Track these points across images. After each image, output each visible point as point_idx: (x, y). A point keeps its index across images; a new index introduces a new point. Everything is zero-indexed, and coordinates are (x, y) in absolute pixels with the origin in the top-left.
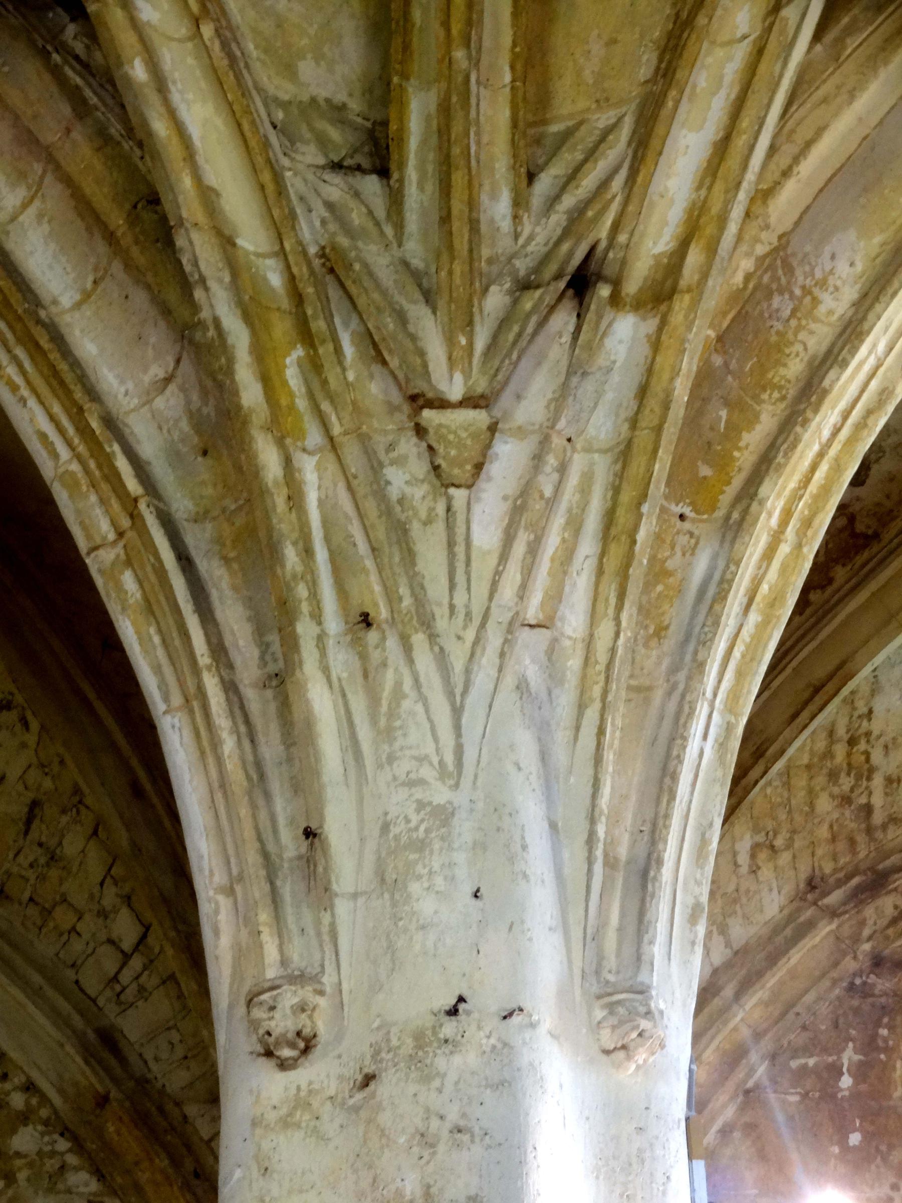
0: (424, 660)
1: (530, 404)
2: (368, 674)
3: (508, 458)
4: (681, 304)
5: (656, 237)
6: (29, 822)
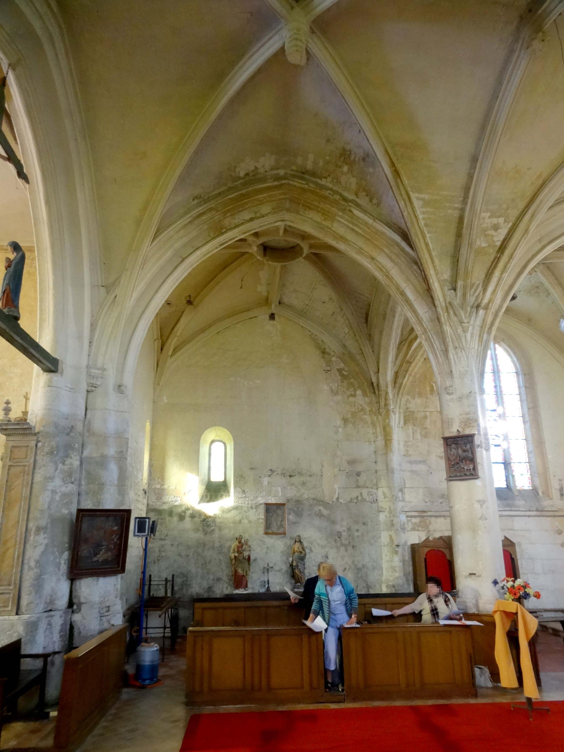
0: (464, 354)
1: (472, 322)
2: (457, 354)
3: (470, 329)
4: (489, 310)
5: (486, 301)
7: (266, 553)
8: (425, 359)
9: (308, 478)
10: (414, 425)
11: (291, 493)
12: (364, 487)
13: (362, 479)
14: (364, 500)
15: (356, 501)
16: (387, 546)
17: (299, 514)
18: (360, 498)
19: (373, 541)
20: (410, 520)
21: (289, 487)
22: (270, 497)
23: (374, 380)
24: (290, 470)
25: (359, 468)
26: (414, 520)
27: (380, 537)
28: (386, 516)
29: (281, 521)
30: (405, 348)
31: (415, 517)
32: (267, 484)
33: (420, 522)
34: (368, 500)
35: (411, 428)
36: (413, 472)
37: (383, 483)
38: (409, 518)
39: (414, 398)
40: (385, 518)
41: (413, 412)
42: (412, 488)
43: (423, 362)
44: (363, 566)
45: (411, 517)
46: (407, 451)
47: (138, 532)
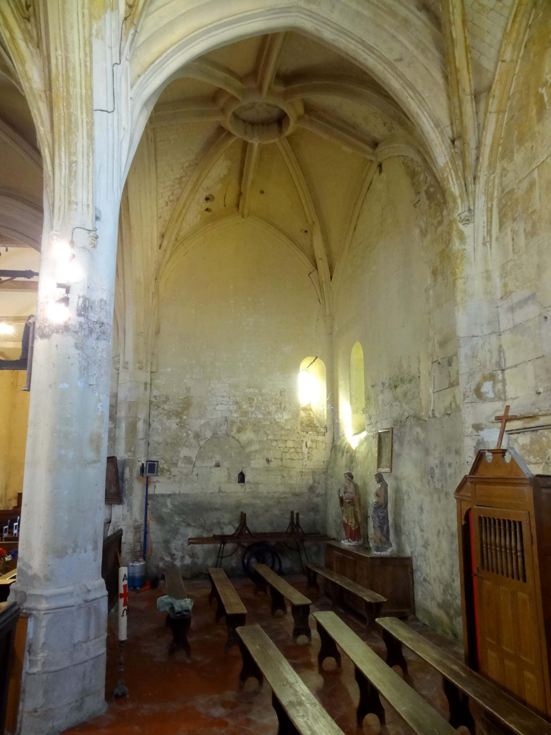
10: (514, 220)
33: (532, 442)
42: (516, 366)
46: (505, 285)
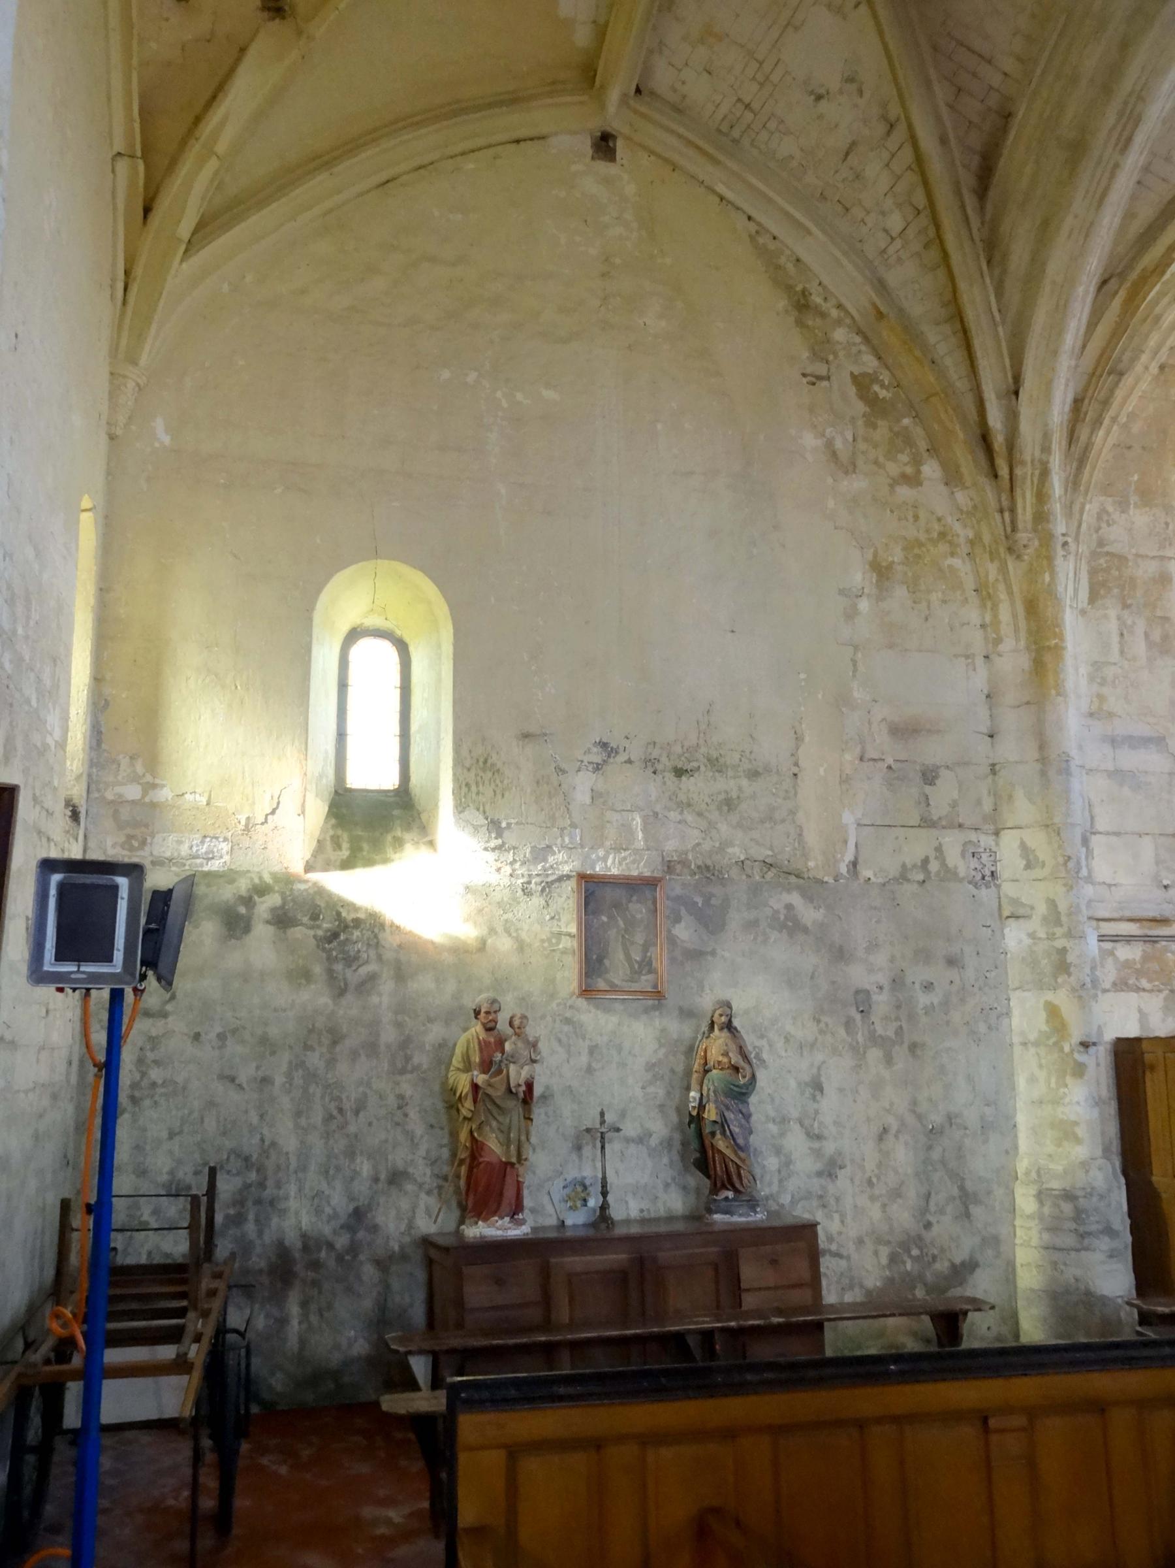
6: (847, 154)
7: (590, 1070)
8: (1162, 368)
9: (744, 782)
10: (1126, 606)
11: (682, 837)
12: (951, 826)
13: (944, 794)
14: (949, 874)
15: (921, 877)
16: (1036, 1044)
17: (711, 920)
18: (934, 866)
19: (982, 1028)
20: (1111, 953)
21: (674, 815)
22: (601, 853)
23: (995, 419)
24: (678, 749)
25: (933, 751)
26: (1124, 952)
27: (1008, 1014)
28: (1032, 935)
29: (646, 948)
30: (1117, 304)
31: (1129, 939)
32: (588, 801)
33: (1146, 958)
34: (962, 872)
35: (1113, 613)
36: (1118, 775)
37: (1023, 809)
38: (1108, 946)
39: (1123, 506)
40: (1027, 941)
41: (1122, 559)
43: (1156, 378)
44: (950, 1118)
45: (1115, 939)
46: (1101, 698)
47: (60, 957)
